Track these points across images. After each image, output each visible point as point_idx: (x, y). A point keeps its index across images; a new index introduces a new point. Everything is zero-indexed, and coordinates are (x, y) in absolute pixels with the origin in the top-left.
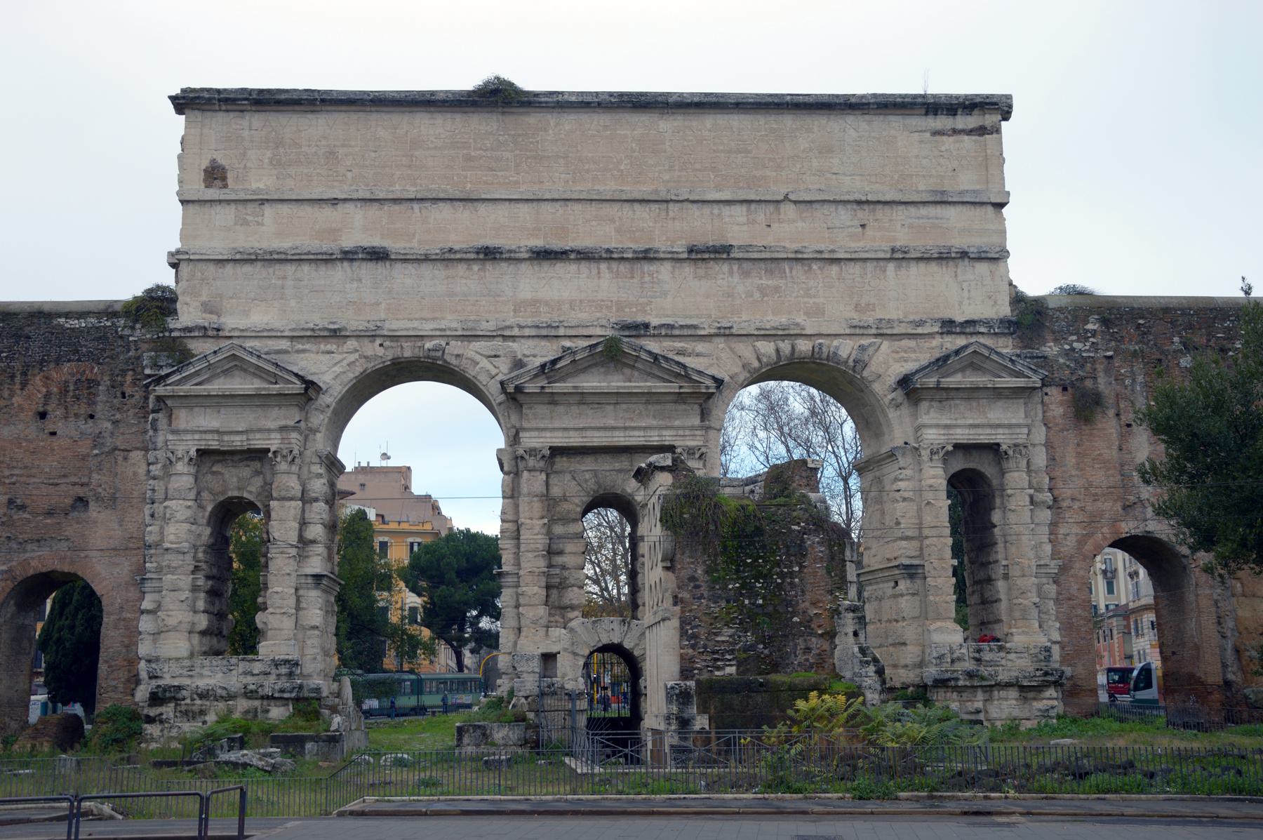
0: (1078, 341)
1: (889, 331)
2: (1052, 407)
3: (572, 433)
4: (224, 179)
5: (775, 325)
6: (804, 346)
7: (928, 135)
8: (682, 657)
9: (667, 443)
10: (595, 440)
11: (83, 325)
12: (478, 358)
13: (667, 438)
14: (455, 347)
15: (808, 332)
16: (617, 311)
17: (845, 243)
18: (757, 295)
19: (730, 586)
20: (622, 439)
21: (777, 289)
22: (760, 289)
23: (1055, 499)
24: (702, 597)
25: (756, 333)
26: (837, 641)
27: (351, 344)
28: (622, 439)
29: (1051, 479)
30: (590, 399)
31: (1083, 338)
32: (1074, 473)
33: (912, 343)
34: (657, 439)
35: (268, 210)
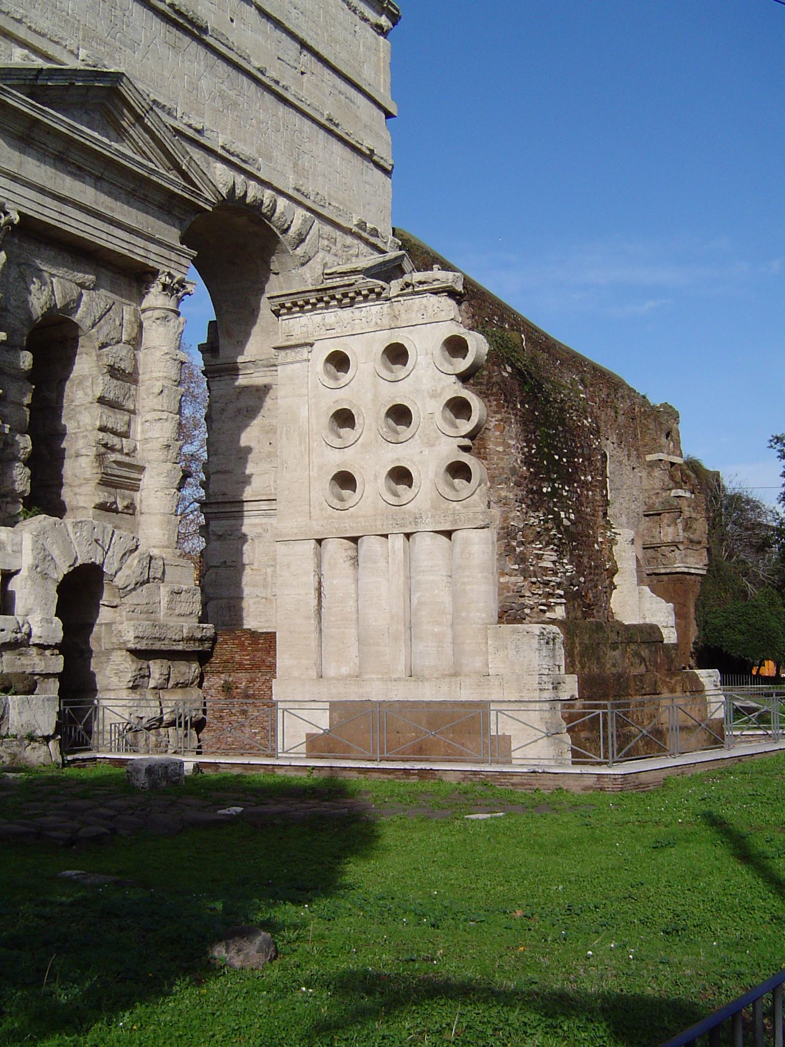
1: (320, 210)
3: (48, 201)
5: (238, 151)
6: (253, 191)
8: (502, 588)
9: (151, 264)
10: (74, 223)
13: (153, 256)
15: (262, 175)
19: (545, 490)
20: (104, 236)
25: (220, 151)
26: (616, 580)
28: (104, 236)
30: (75, 156)
34: (142, 252)
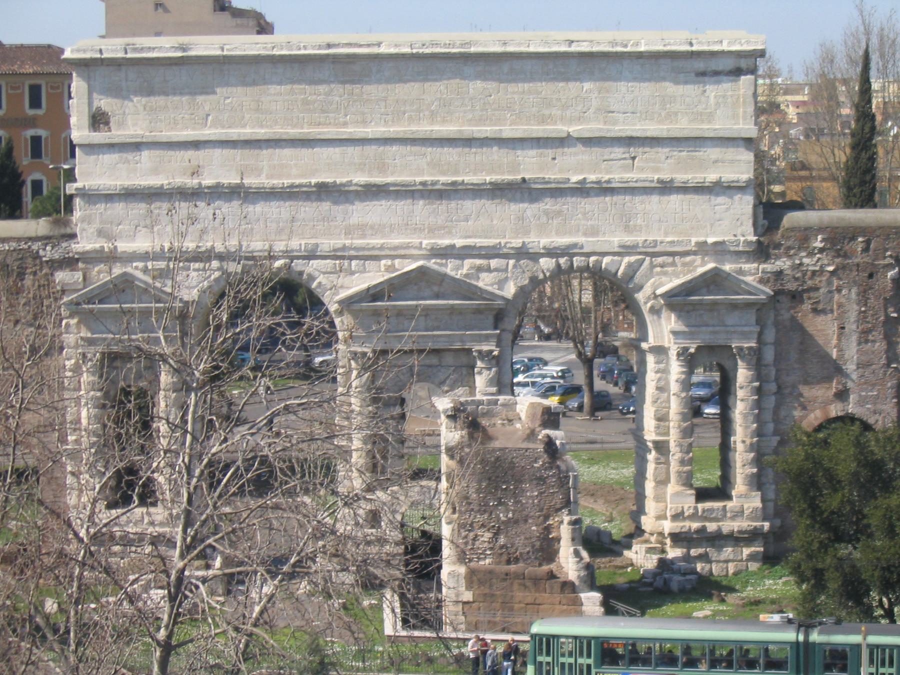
0: (806, 256)
2: (783, 312)
4: (107, 123)
7: (693, 74)
11: (7, 248)
12: (317, 274)
14: (298, 265)
16: (429, 232)
17: (617, 175)
18: (544, 219)
21: (559, 213)
22: (546, 213)
23: (779, 387)
24: (472, 510)
27: (215, 264)
29: (777, 371)
31: (811, 254)
32: (796, 366)
33: (670, 259)
35: (145, 154)
